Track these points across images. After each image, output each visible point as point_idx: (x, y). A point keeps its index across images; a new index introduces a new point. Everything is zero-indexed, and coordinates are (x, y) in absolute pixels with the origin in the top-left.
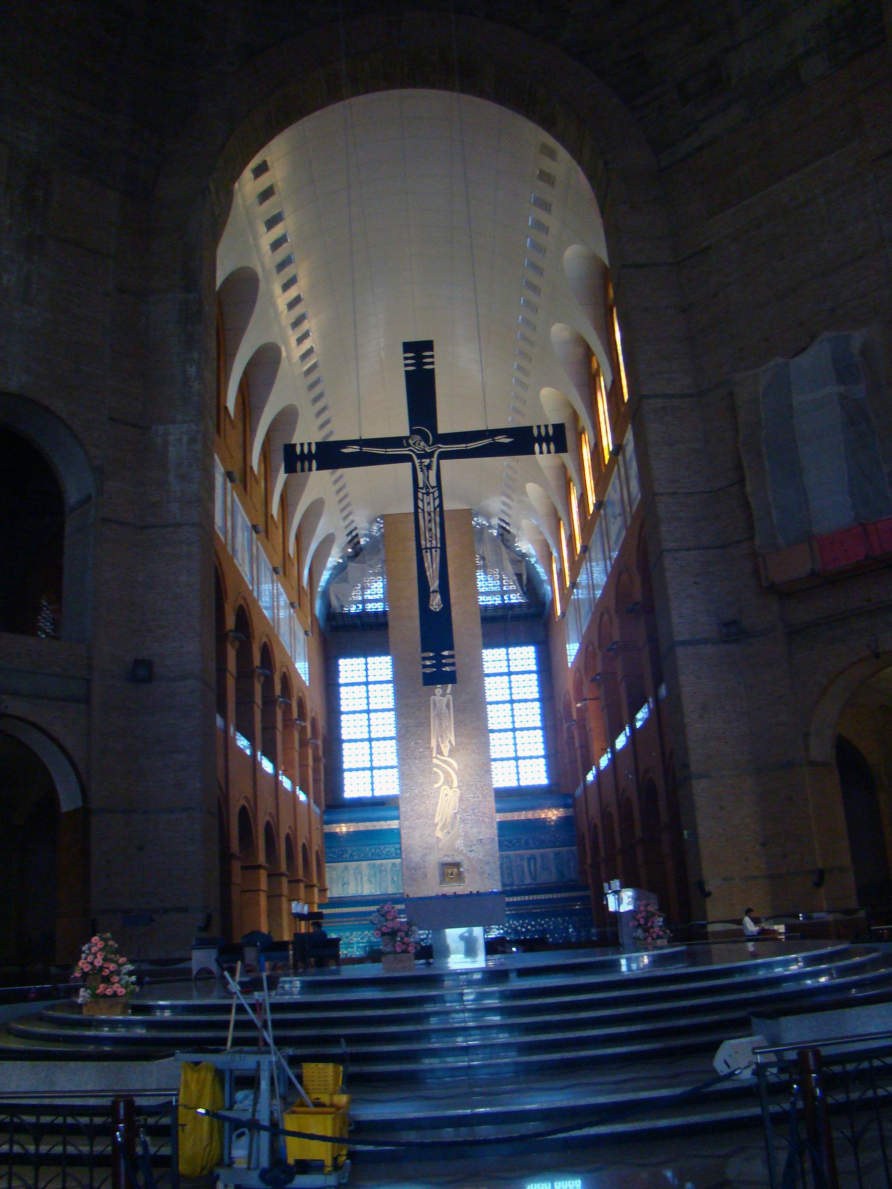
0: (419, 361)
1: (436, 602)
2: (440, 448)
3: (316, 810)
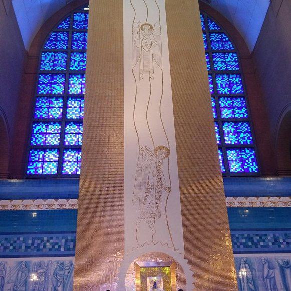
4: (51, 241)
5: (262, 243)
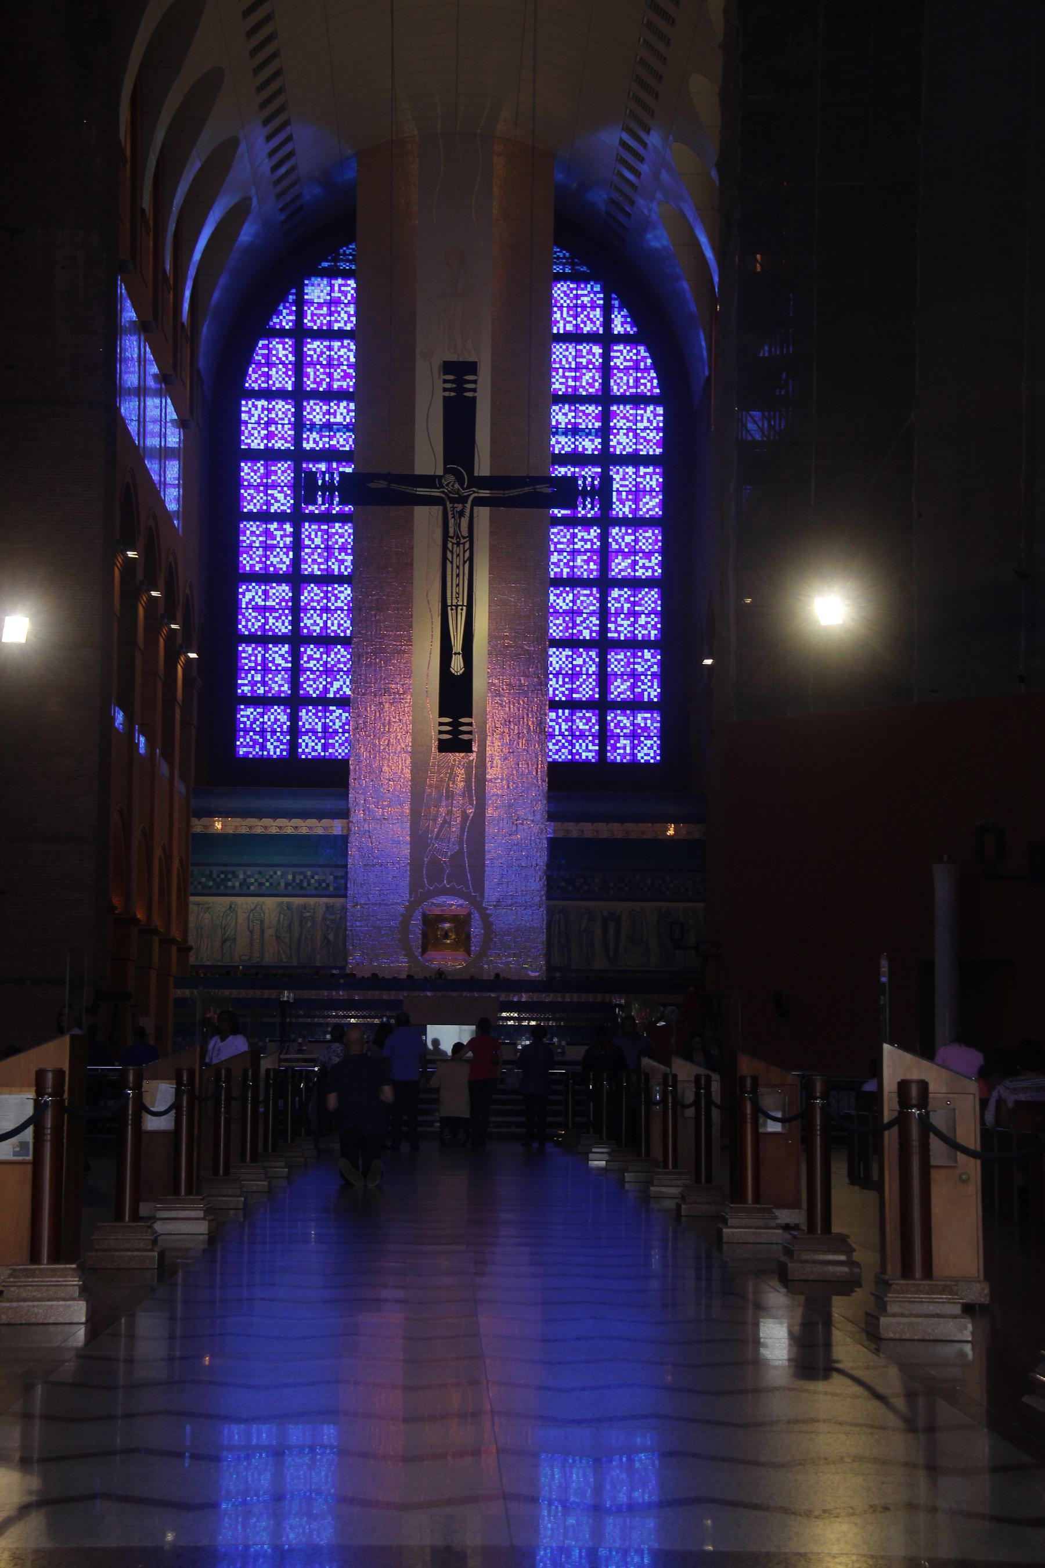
0: (460, 385)
1: (457, 665)
2: (474, 492)
3: (180, 787)
4: (316, 877)
5: (585, 888)
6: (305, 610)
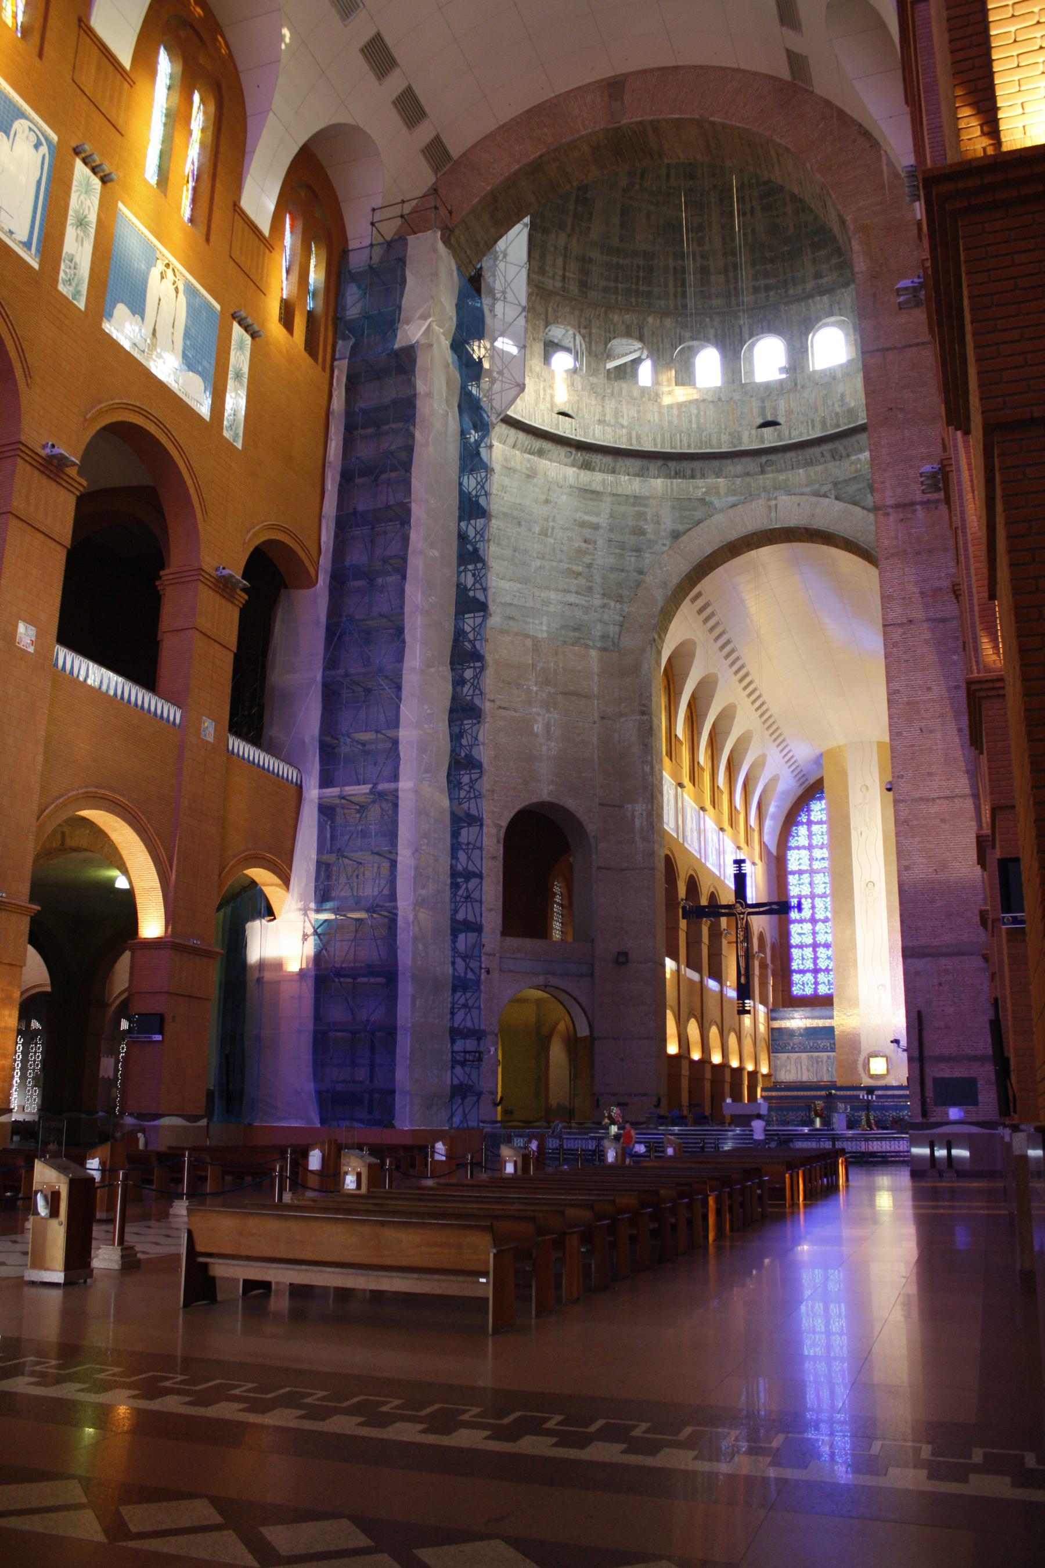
6: (817, 933)
